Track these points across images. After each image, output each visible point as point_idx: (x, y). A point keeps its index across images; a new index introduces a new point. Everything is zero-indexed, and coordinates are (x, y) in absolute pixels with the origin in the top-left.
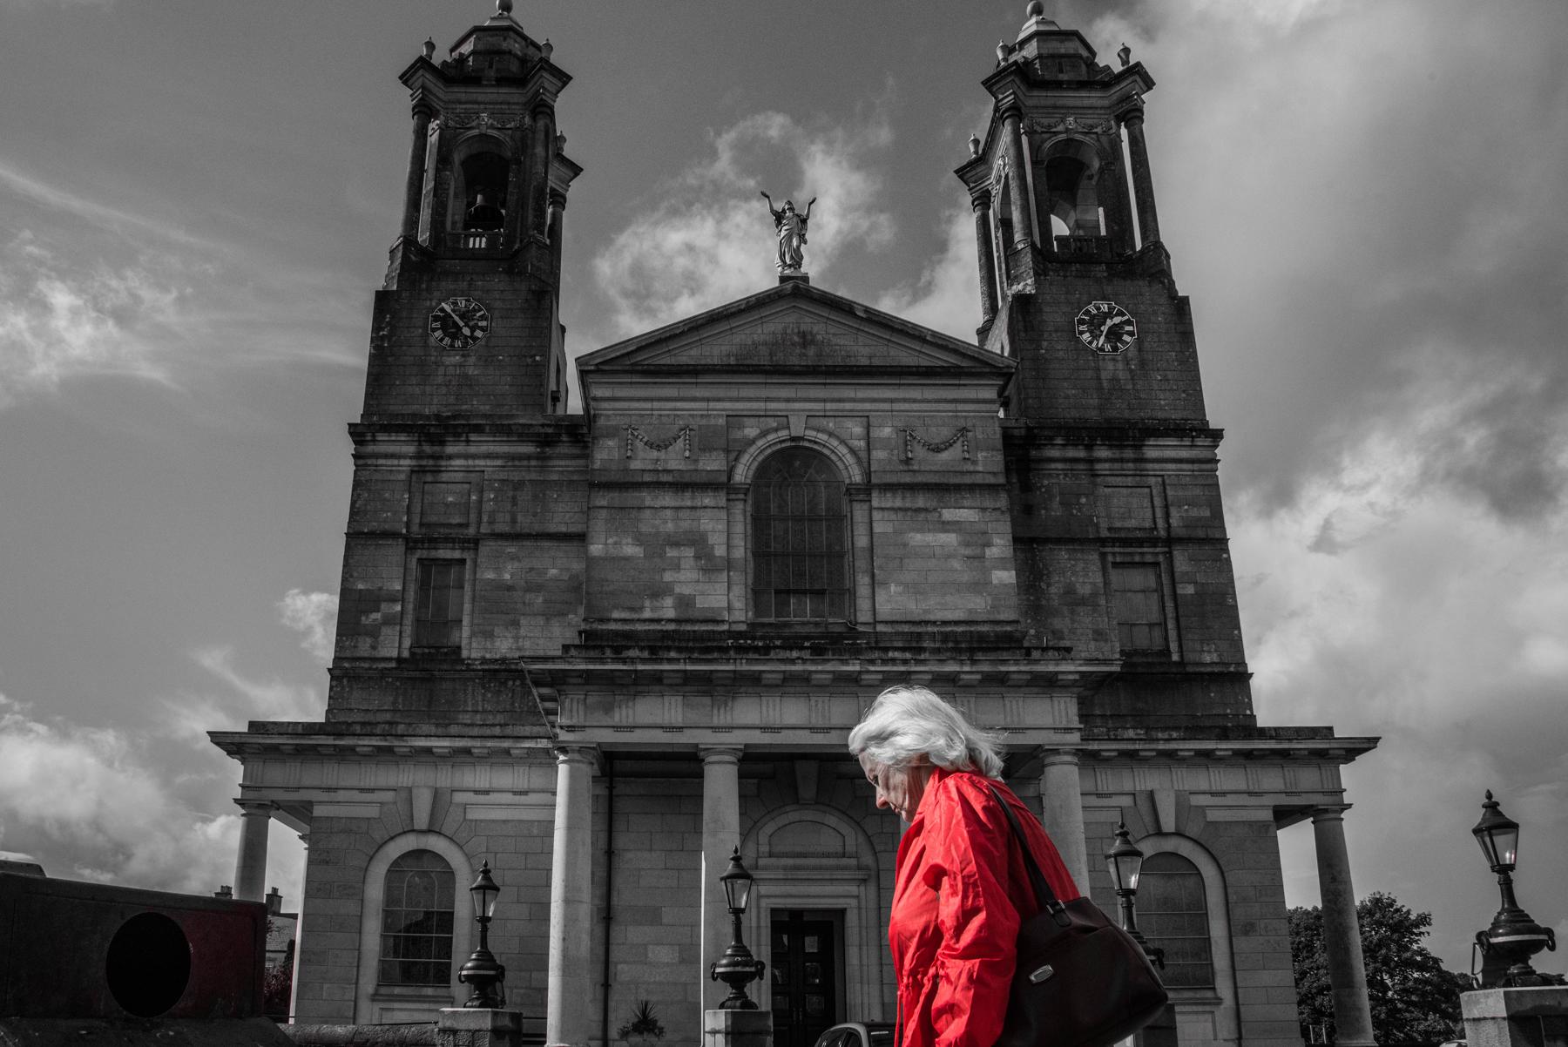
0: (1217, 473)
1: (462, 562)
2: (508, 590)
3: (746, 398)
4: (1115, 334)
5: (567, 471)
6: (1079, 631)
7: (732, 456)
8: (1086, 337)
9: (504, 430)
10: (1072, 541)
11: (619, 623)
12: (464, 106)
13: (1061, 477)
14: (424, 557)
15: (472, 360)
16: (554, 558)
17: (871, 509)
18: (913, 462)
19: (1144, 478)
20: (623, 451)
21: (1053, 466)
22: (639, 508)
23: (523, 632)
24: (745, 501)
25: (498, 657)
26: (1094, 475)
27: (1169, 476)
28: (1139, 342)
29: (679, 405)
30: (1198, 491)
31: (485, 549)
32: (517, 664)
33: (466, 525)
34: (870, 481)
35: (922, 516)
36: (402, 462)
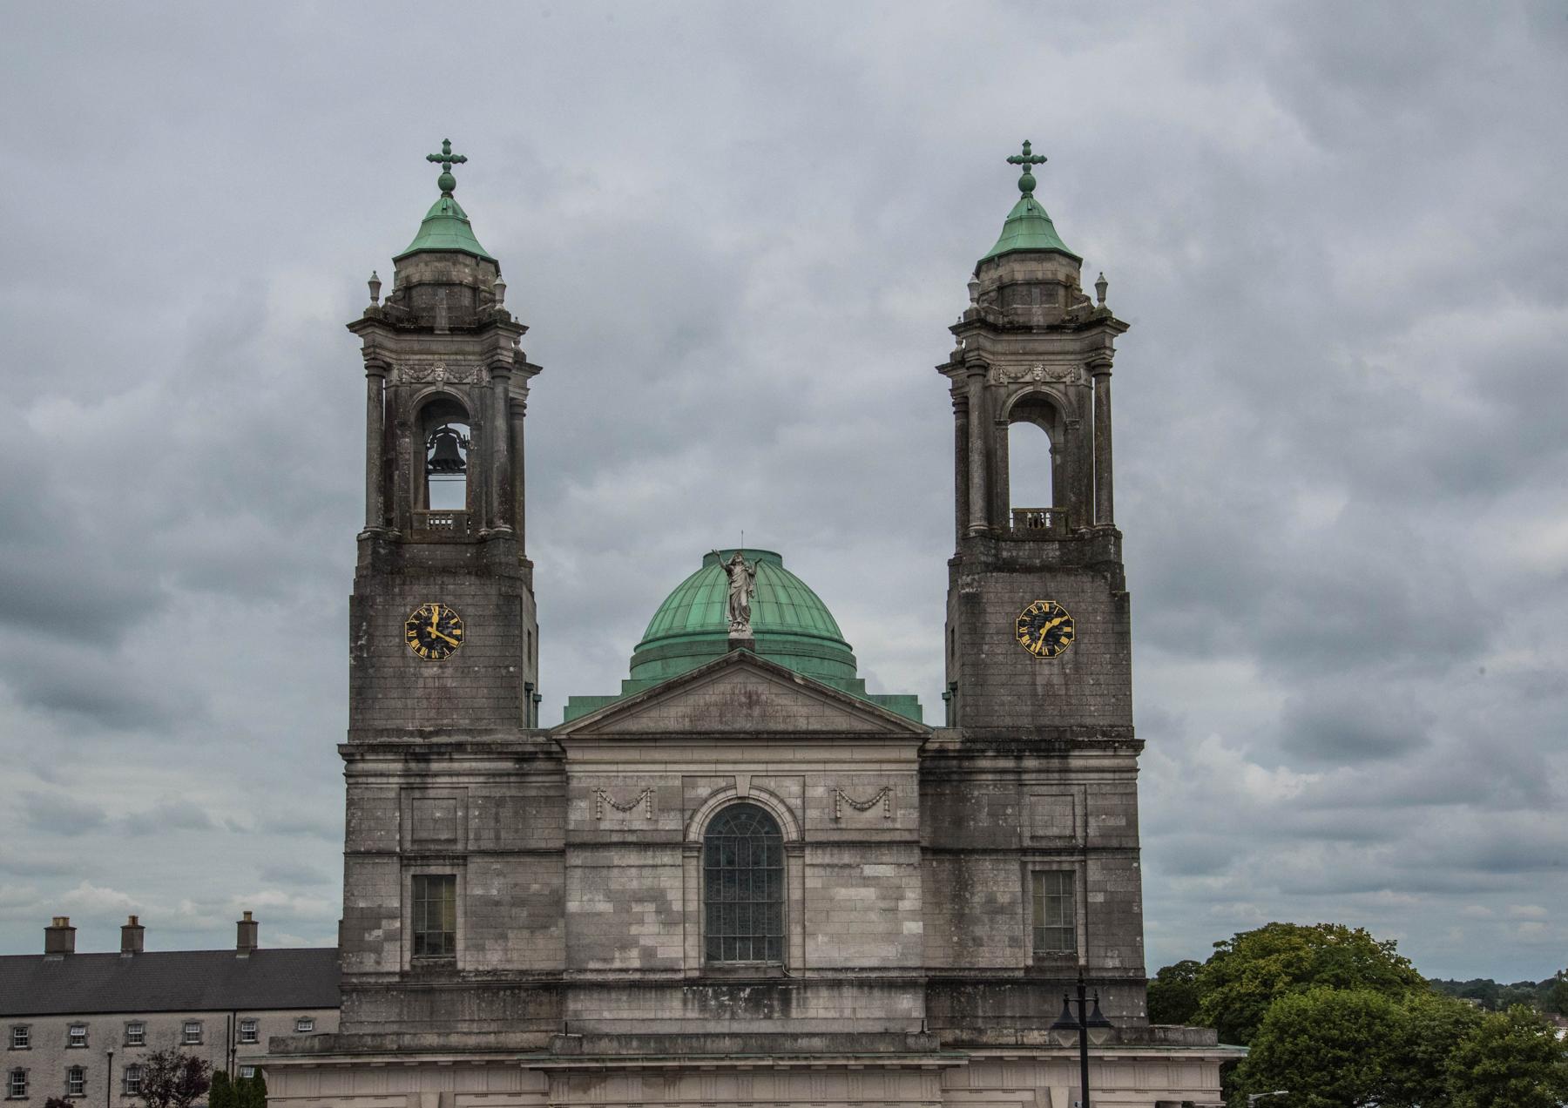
0: (1137, 781)
1: (451, 879)
2: (496, 905)
3: (700, 761)
4: (1053, 637)
5: (544, 787)
6: (997, 938)
7: (688, 814)
8: (1026, 639)
9: (486, 750)
10: (996, 851)
11: (595, 973)
12: (418, 357)
13: (991, 788)
14: (418, 873)
15: (449, 671)
16: (536, 873)
17: (805, 865)
18: (841, 820)
19: (1067, 787)
20: (594, 813)
21: (984, 777)
22: (609, 867)
23: (510, 944)
24: (698, 857)
25: (489, 968)
26: (1021, 784)
27: (1091, 784)
28: (1077, 643)
29: (641, 767)
30: (1116, 800)
31: (475, 865)
32: (506, 975)
33: (454, 841)
34: (803, 839)
35: (847, 872)
36: (391, 780)
